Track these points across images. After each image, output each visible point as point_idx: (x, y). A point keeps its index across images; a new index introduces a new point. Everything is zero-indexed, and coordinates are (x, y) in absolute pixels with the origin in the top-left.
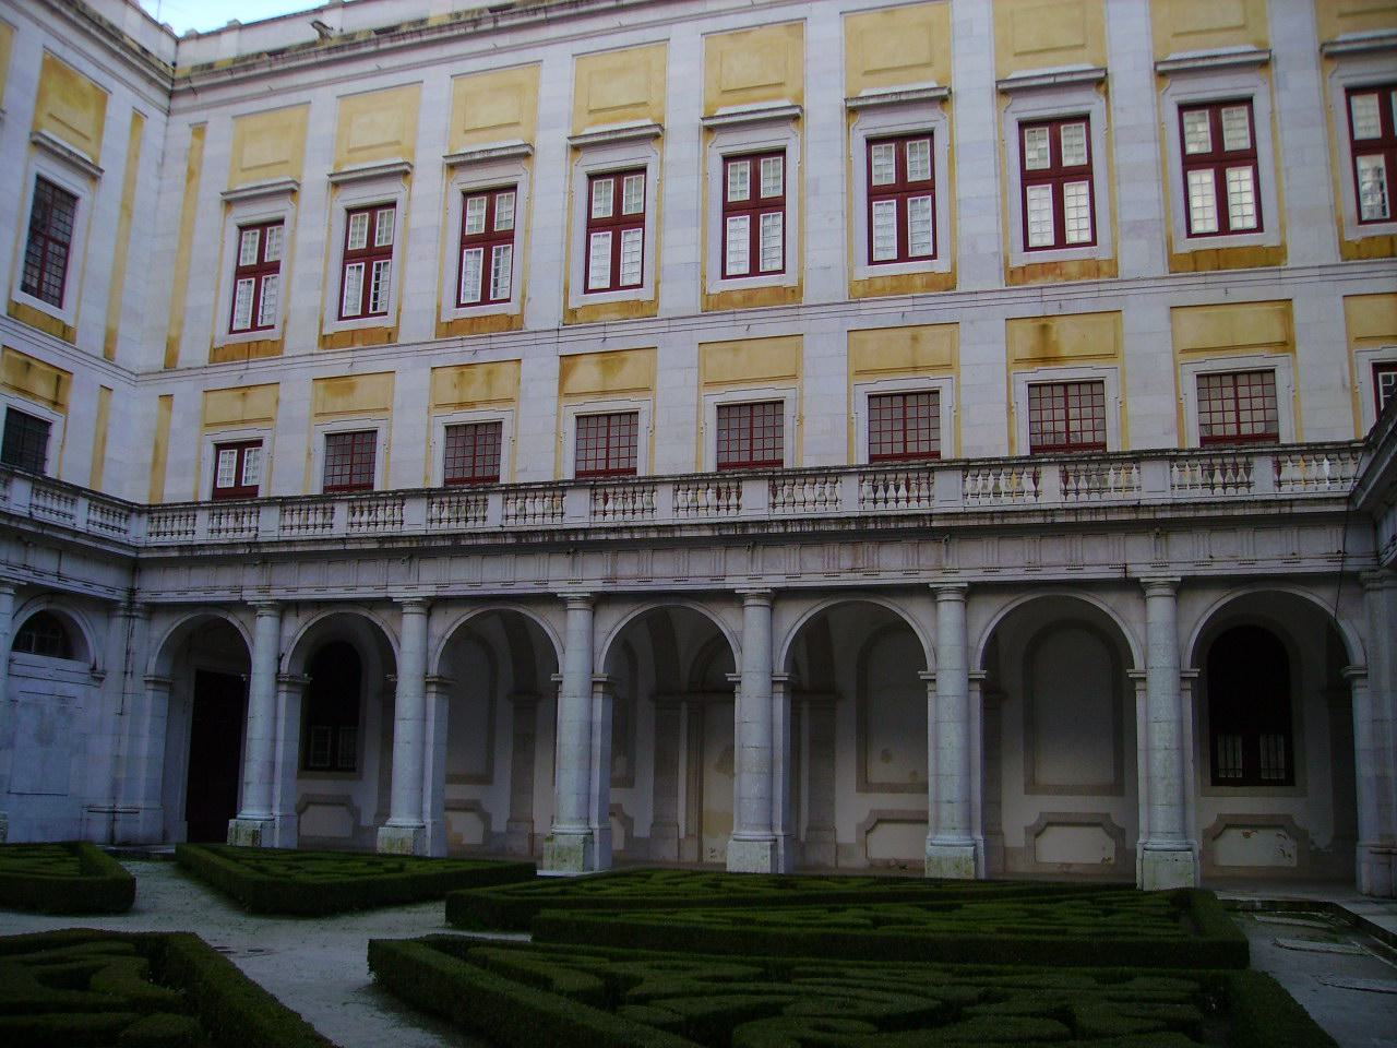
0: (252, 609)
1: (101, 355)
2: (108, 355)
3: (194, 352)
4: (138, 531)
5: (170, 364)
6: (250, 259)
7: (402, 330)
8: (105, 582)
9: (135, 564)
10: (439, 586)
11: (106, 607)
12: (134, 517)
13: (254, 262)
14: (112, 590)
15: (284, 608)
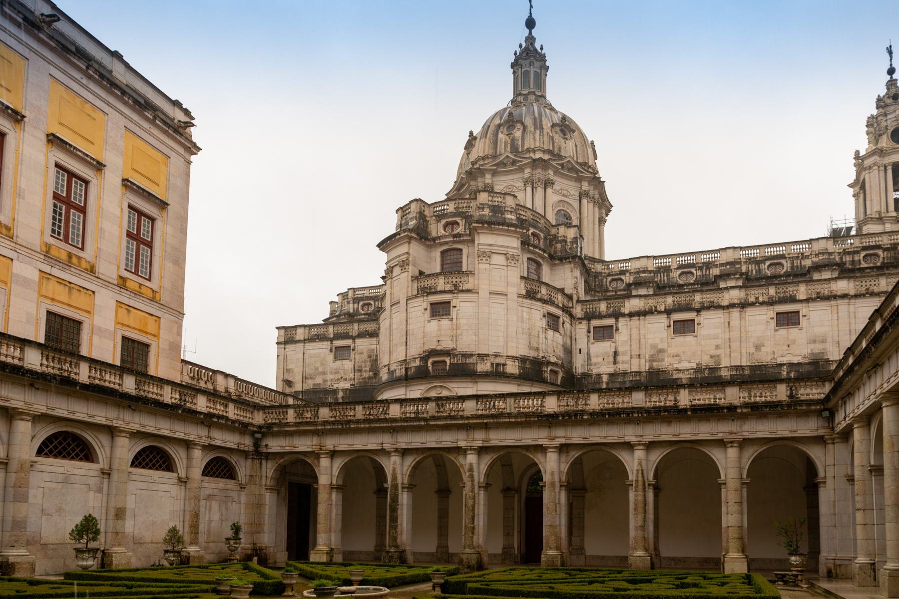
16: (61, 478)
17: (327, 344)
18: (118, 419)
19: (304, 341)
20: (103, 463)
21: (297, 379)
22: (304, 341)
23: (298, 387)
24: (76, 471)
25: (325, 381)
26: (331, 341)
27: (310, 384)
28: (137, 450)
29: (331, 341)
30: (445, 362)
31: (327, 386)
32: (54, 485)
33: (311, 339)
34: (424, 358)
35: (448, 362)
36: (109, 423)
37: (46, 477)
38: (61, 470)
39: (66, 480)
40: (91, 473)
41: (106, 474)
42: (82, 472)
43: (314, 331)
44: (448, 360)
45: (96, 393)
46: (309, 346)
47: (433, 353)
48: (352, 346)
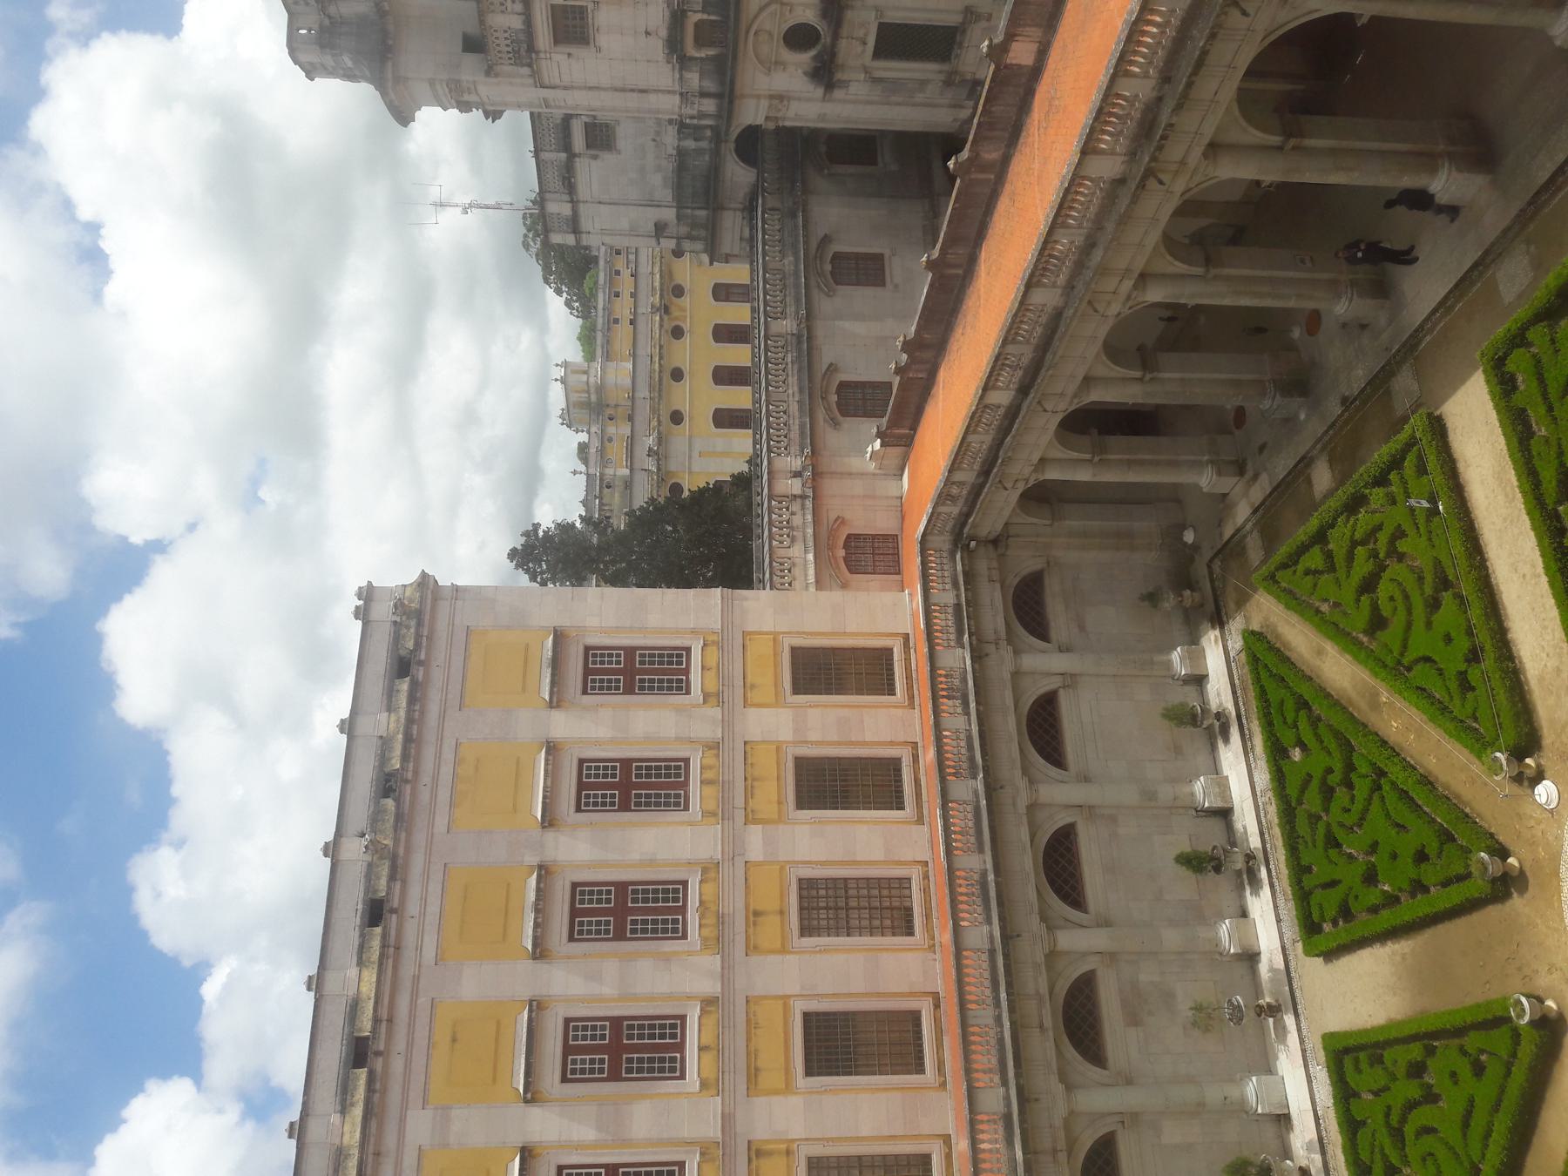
17: (581, 165)
19: (574, 203)
21: (653, 215)
22: (574, 203)
23: (669, 214)
25: (659, 169)
26: (575, 155)
27: (667, 195)
28: (1042, 761)
29: (575, 155)
30: (698, 25)
31: (669, 166)
33: (570, 186)
34: (683, 62)
35: (699, 16)
43: (555, 182)
44: (694, 18)
46: (583, 191)
47: (674, 45)
48: (585, 119)
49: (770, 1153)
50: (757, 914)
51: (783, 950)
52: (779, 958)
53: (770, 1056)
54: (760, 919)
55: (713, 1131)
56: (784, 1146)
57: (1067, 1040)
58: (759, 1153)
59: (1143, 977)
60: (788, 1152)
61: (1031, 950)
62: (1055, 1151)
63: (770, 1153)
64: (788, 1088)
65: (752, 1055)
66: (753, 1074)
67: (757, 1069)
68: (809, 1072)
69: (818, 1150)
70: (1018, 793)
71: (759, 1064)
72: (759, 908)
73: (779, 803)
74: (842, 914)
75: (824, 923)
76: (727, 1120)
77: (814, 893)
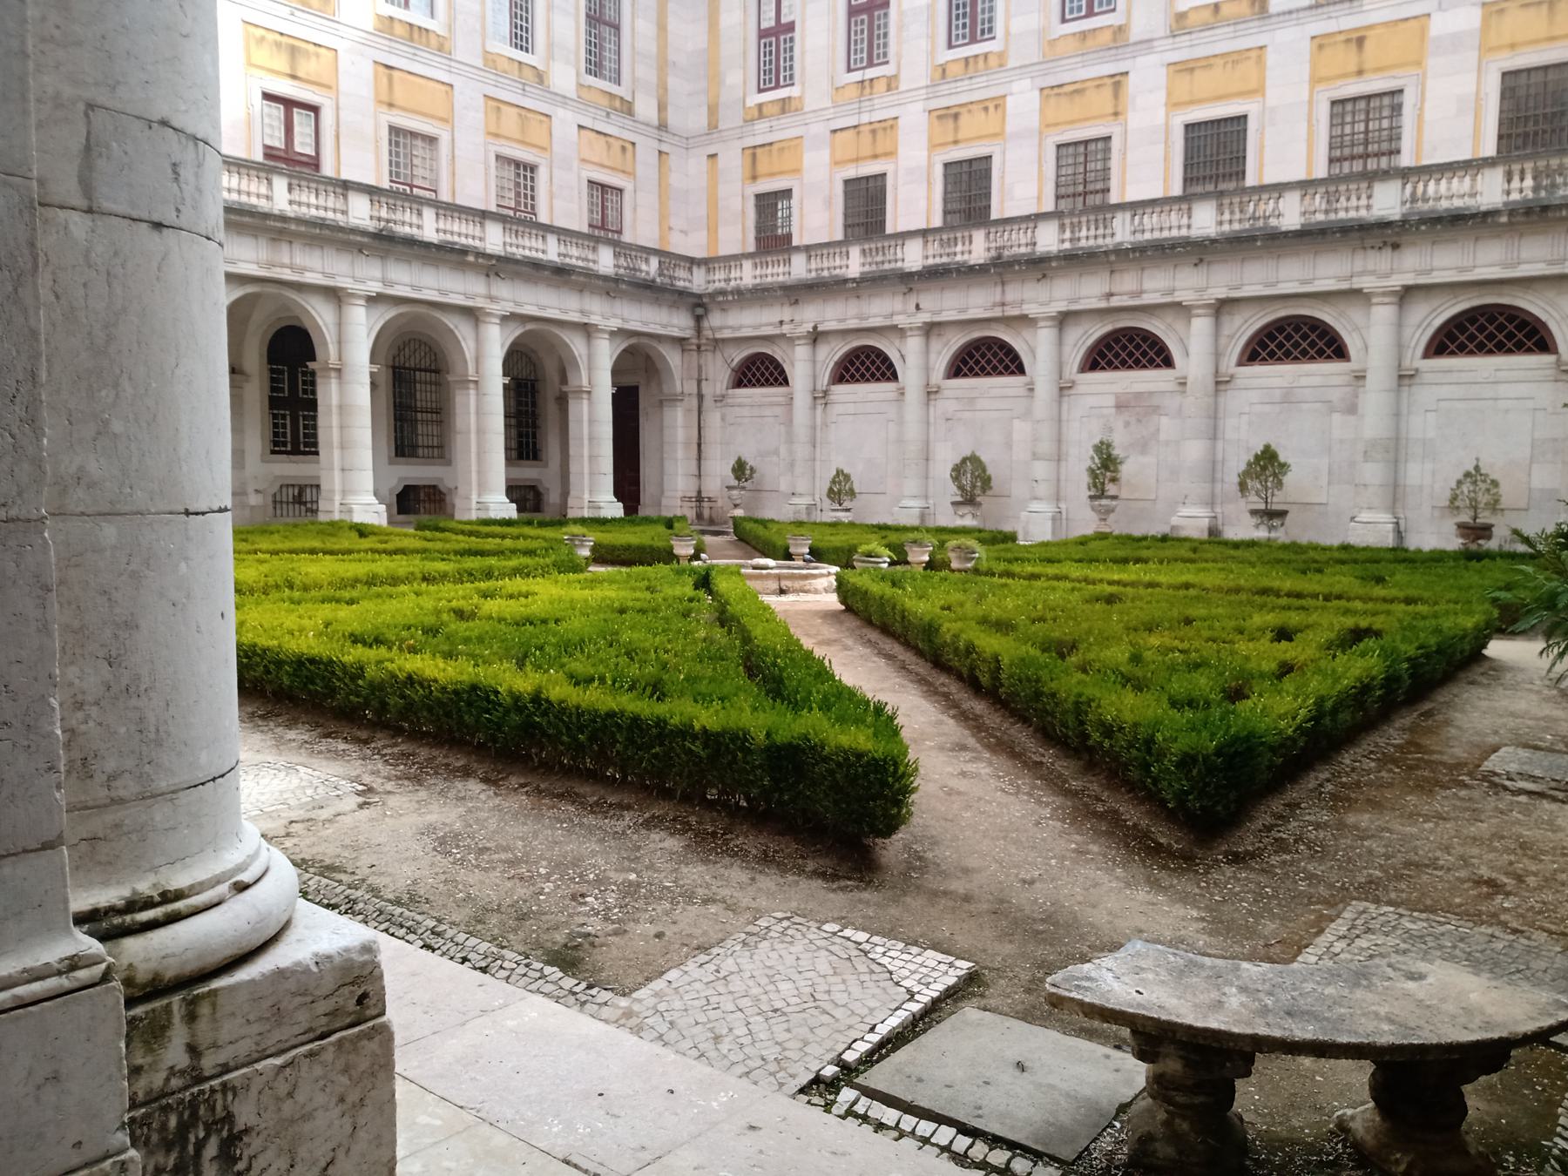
0: (790, 340)
1: (656, 122)
2: (662, 126)
3: (730, 119)
4: (698, 281)
5: (713, 126)
6: (769, 22)
7: (903, 76)
8: (676, 323)
9: (699, 306)
10: (934, 313)
11: (680, 342)
12: (695, 269)
13: (773, 23)
14: (681, 329)
15: (816, 337)
16: (1277, 394)
18: (1363, 273)
20: (1354, 365)
24: (1304, 381)
32: (1267, 408)
36: (1344, 286)
37: (1253, 396)
38: (1277, 382)
39: (1288, 399)
40: (1336, 380)
41: (1360, 377)
42: (1316, 381)
45: (1313, 237)
49: (1116, 95)
50: (1360, 41)
51: (1316, 80)
52: (1306, 77)
53: (1203, 82)
54: (1353, 46)
55: (1136, 33)
56: (1120, 109)
57: (1108, 328)
58: (1117, 86)
59: (1164, 420)
60: (1116, 114)
61: (1186, 284)
62: (1003, 304)
63: (1116, 95)
64: (1173, 104)
65: (1206, 63)
66: (1184, 68)
67: (1192, 70)
68: (1189, 127)
69: (1115, 144)
70: (1381, 271)
71: (1197, 73)
72: (1368, 44)
73: (1513, 46)
74: (1360, 150)
75: (1348, 129)
76: (1147, 44)
77: (1386, 113)
